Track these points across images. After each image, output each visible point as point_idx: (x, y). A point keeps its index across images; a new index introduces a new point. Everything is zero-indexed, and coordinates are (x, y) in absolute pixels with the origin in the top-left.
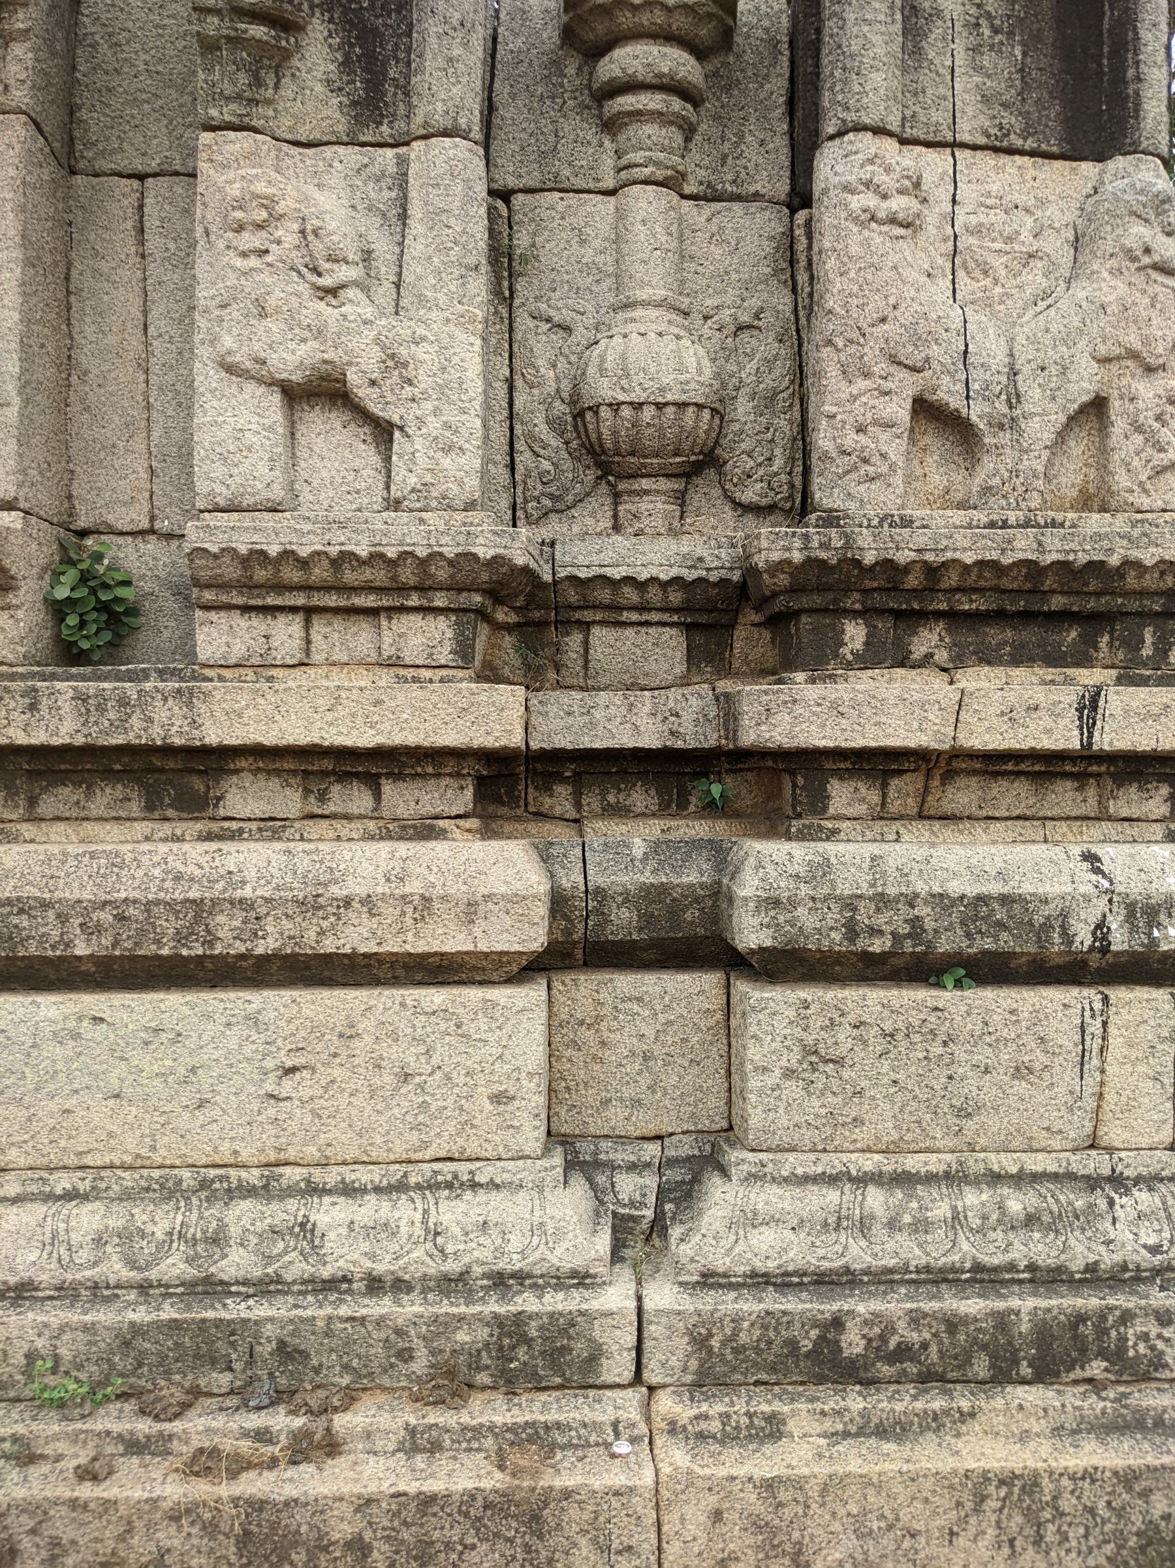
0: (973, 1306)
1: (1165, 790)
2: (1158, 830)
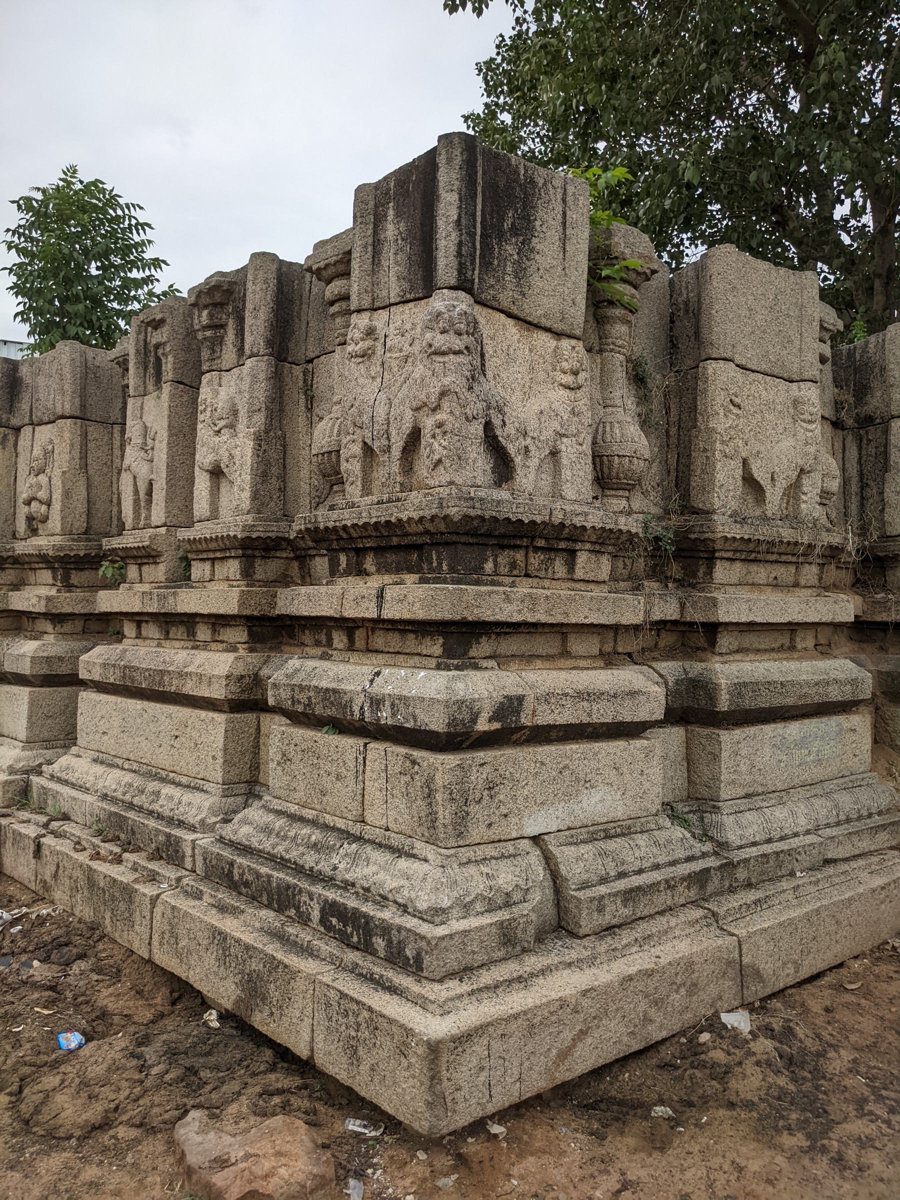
0: (264, 870)
1: (441, 641)
2: (433, 662)
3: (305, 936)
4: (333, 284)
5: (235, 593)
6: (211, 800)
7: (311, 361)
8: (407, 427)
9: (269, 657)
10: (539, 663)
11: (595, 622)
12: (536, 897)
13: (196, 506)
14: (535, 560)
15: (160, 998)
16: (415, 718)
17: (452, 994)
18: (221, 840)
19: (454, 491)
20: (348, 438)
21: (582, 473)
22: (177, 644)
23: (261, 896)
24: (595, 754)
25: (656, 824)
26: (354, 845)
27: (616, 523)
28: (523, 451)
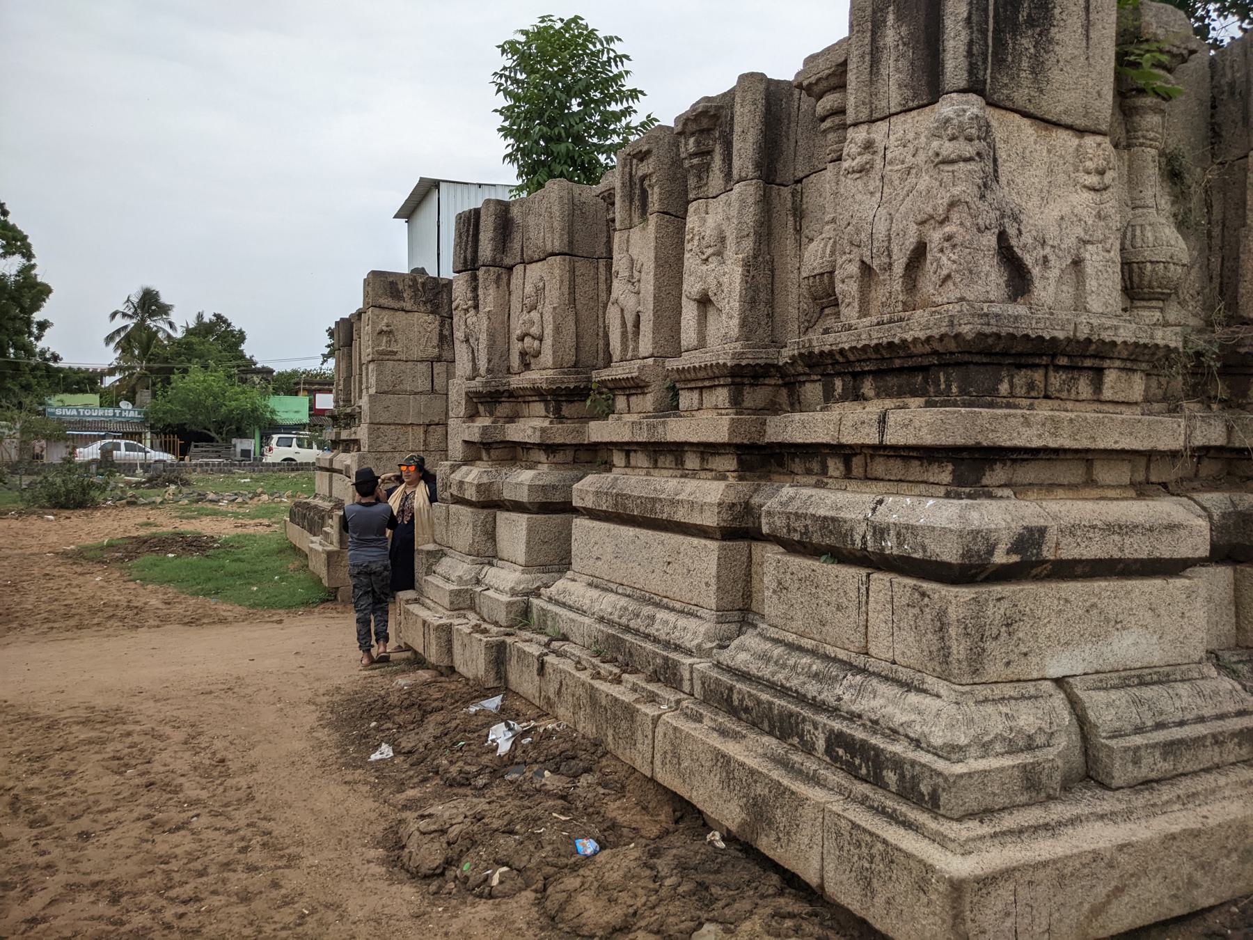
0: (765, 697)
1: (950, 467)
2: (942, 490)
3: (811, 765)
4: (824, 99)
5: (725, 422)
6: (707, 626)
7: (800, 181)
8: (911, 242)
9: (759, 485)
10: (1060, 493)
11: (1127, 447)
12: (1061, 742)
13: (683, 336)
14: (1056, 380)
15: (665, 815)
16: (924, 549)
17: (972, 834)
18: (718, 665)
19: (965, 307)
20: (844, 258)
21: (1109, 283)
22: (665, 472)
23: (762, 722)
24: (1128, 593)
25: (1200, 672)
26: (858, 677)
27: (1152, 337)
28: (1041, 262)
